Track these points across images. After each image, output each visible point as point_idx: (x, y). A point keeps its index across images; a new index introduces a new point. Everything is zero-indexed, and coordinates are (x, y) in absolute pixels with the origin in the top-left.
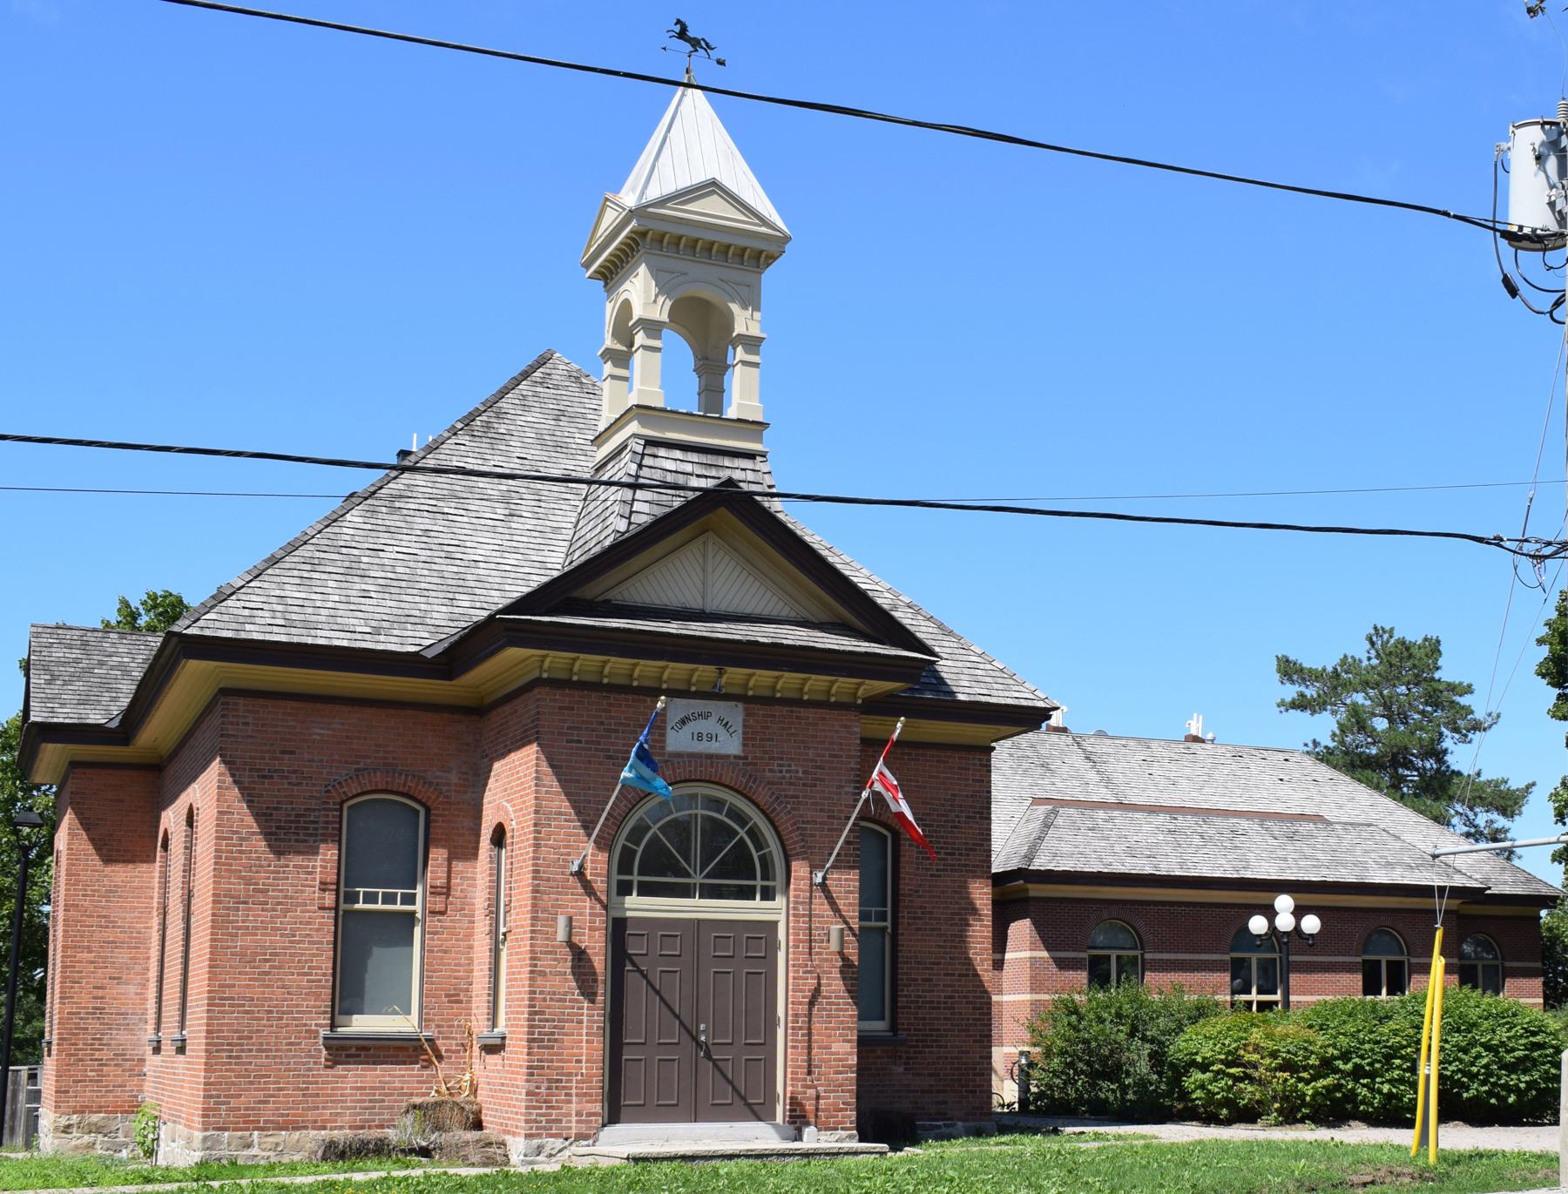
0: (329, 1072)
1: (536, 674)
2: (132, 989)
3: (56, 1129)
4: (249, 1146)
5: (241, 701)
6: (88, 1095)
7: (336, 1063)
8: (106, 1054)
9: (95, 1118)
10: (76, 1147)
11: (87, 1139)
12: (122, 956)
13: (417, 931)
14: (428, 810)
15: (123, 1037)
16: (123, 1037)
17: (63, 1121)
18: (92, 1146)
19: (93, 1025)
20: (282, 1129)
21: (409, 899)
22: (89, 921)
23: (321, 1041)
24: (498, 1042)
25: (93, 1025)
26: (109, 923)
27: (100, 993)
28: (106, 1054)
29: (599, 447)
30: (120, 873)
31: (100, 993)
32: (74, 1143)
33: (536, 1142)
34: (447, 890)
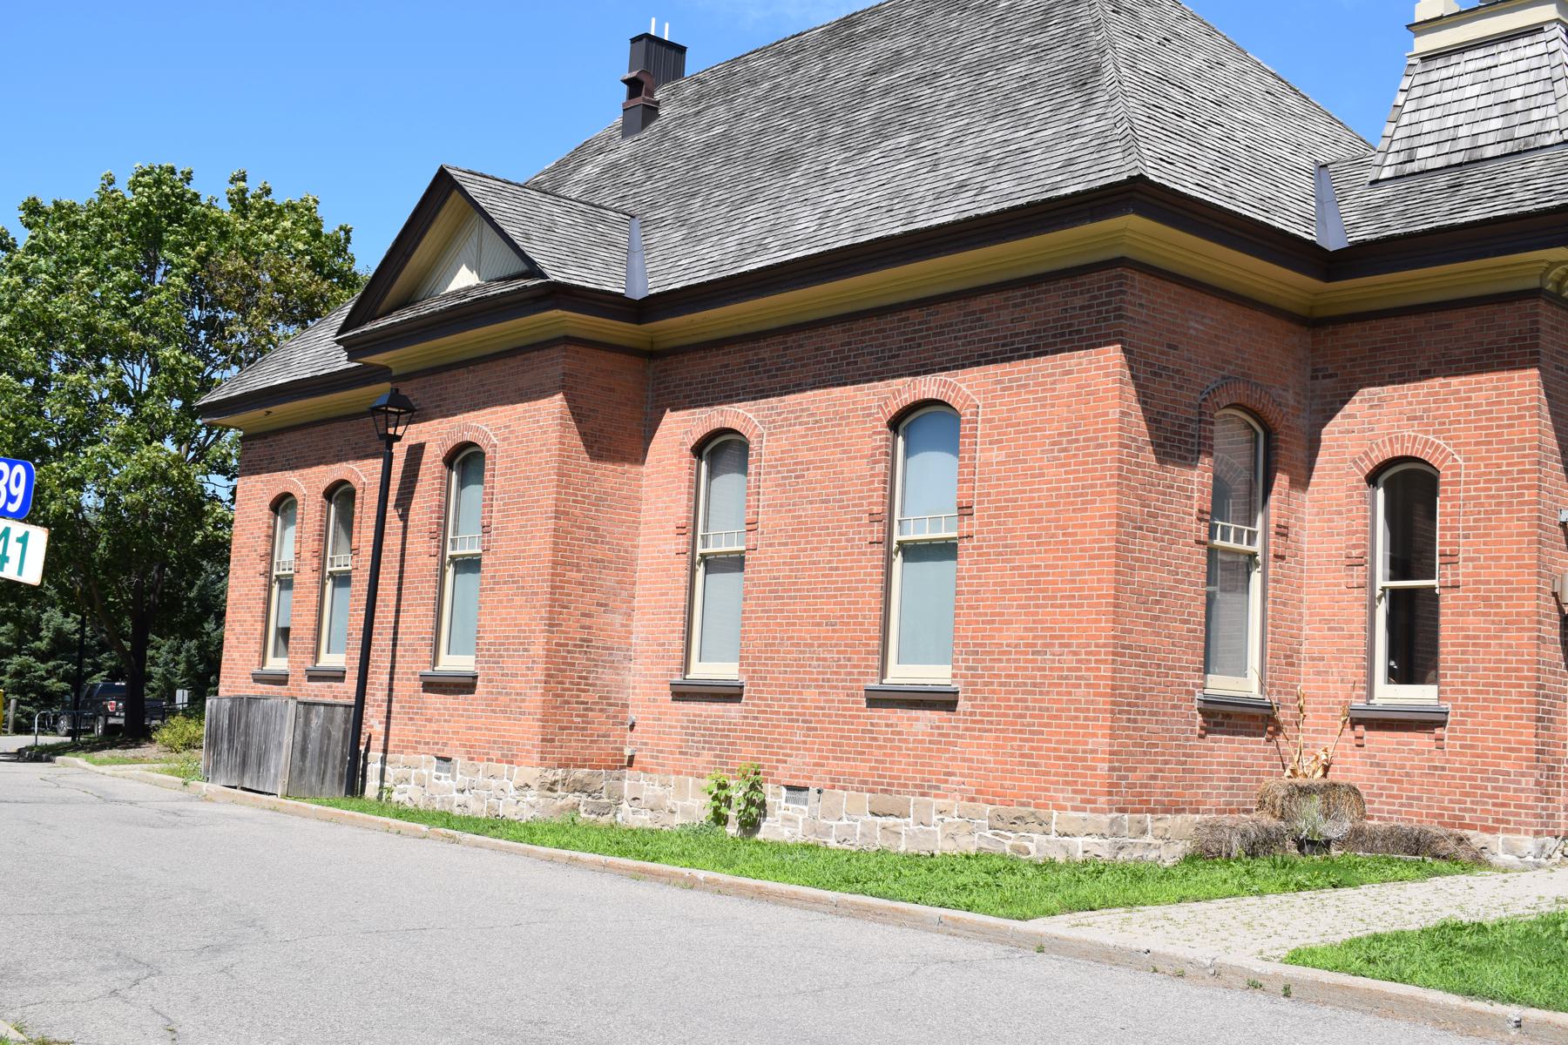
0: (1202, 743)
1: (1534, 283)
2: (618, 619)
3: (542, 786)
4: (1144, 832)
5: (1137, 276)
6: (573, 745)
7: (1208, 732)
8: (591, 697)
9: (580, 773)
10: (562, 809)
11: (572, 798)
12: (610, 579)
13: (1256, 577)
14: (1269, 433)
15: (607, 676)
16: (607, 676)
17: (550, 776)
18: (575, 808)
19: (580, 660)
20: (1167, 811)
21: (1252, 537)
22: (578, 533)
23: (1196, 704)
24: (736, 691)
25: (580, 660)
26: (597, 538)
27: (587, 621)
28: (591, 697)
29: (1417, 34)
30: (610, 475)
31: (587, 621)
32: (559, 803)
33: (1541, 840)
34: (1283, 531)
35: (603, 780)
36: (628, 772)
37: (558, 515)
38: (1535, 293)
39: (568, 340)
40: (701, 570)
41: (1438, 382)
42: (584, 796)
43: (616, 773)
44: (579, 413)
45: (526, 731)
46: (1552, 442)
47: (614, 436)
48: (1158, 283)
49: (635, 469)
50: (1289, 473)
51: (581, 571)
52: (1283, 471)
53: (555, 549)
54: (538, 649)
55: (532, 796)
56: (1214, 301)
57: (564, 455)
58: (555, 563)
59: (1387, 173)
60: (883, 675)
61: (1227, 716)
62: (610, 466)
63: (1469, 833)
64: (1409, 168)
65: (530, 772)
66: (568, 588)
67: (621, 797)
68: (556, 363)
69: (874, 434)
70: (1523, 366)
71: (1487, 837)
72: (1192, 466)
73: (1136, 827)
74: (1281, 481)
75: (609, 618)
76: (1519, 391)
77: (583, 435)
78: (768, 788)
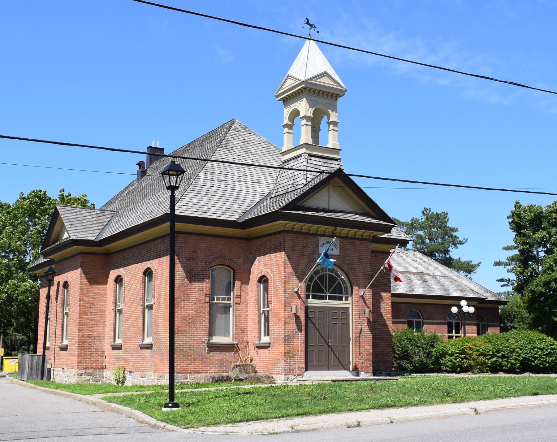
0: (208, 355)
1: (283, 229)
2: (100, 328)
3: (78, 375)
4: (186, 378)
5: (181, 235)
6: (88, 363)
7: (210, 352)
8: (92, 350)
9: (90, 371)
10: (85, 381)
11: (88, 378)
12: (98, 317)
13: (231, 309)
14: (234, 271)
15: (98, 344)
16: (98, 344)
17: (80, 372)
18: (89, 380)
19: (89, 340)
20: (195, 373)
21: (229, 299)
22: (87, 305)
23: (206, 345)
25: (89, 340)
26: (93, 306)
27: (91, 329)
28: (92, 350)
29: (283, 155)
30: (96, 289)
31: (91, 329)
32: (84, 379)
33: (287, 376)
34: (239, 297)
35: (98, 372)
36: (105, 370)
37: (80, 301)
38: (284, 231)
39: (82, 253)
40: (118, 314)
41: (269, 255)
42: (91, 377)
43: (101, 370)
44: (86, 273)
45: (75, 360)
46: (291, 270)
47: (96, 277)
48: (187, 236)
49: (104, 286)
50: (240, 281)
51: (89, 315)
52: (238, 280)
53: (80, 310)
54: (77, 338)
55: (76, 377)
56: (210, 238)
57: (82, 284)
58: (80, 314)
59: (273, 196)
60: (143, 341)
61: (219, 347)
62: (97, 286)
63: (273, 375)
64: (277, 194)
65: (75, 371)
66: (84, 321)
67: (103, 377)
68: (79, 260)
69: (140, 276)
70: (280, 251)
71: (276, 376)
72: (203, 282)
73: (183, 377)
74: (238, 283)
75: (97, 328)
76: (280, 257)
77: (87, 279)
78: (126, 372)
